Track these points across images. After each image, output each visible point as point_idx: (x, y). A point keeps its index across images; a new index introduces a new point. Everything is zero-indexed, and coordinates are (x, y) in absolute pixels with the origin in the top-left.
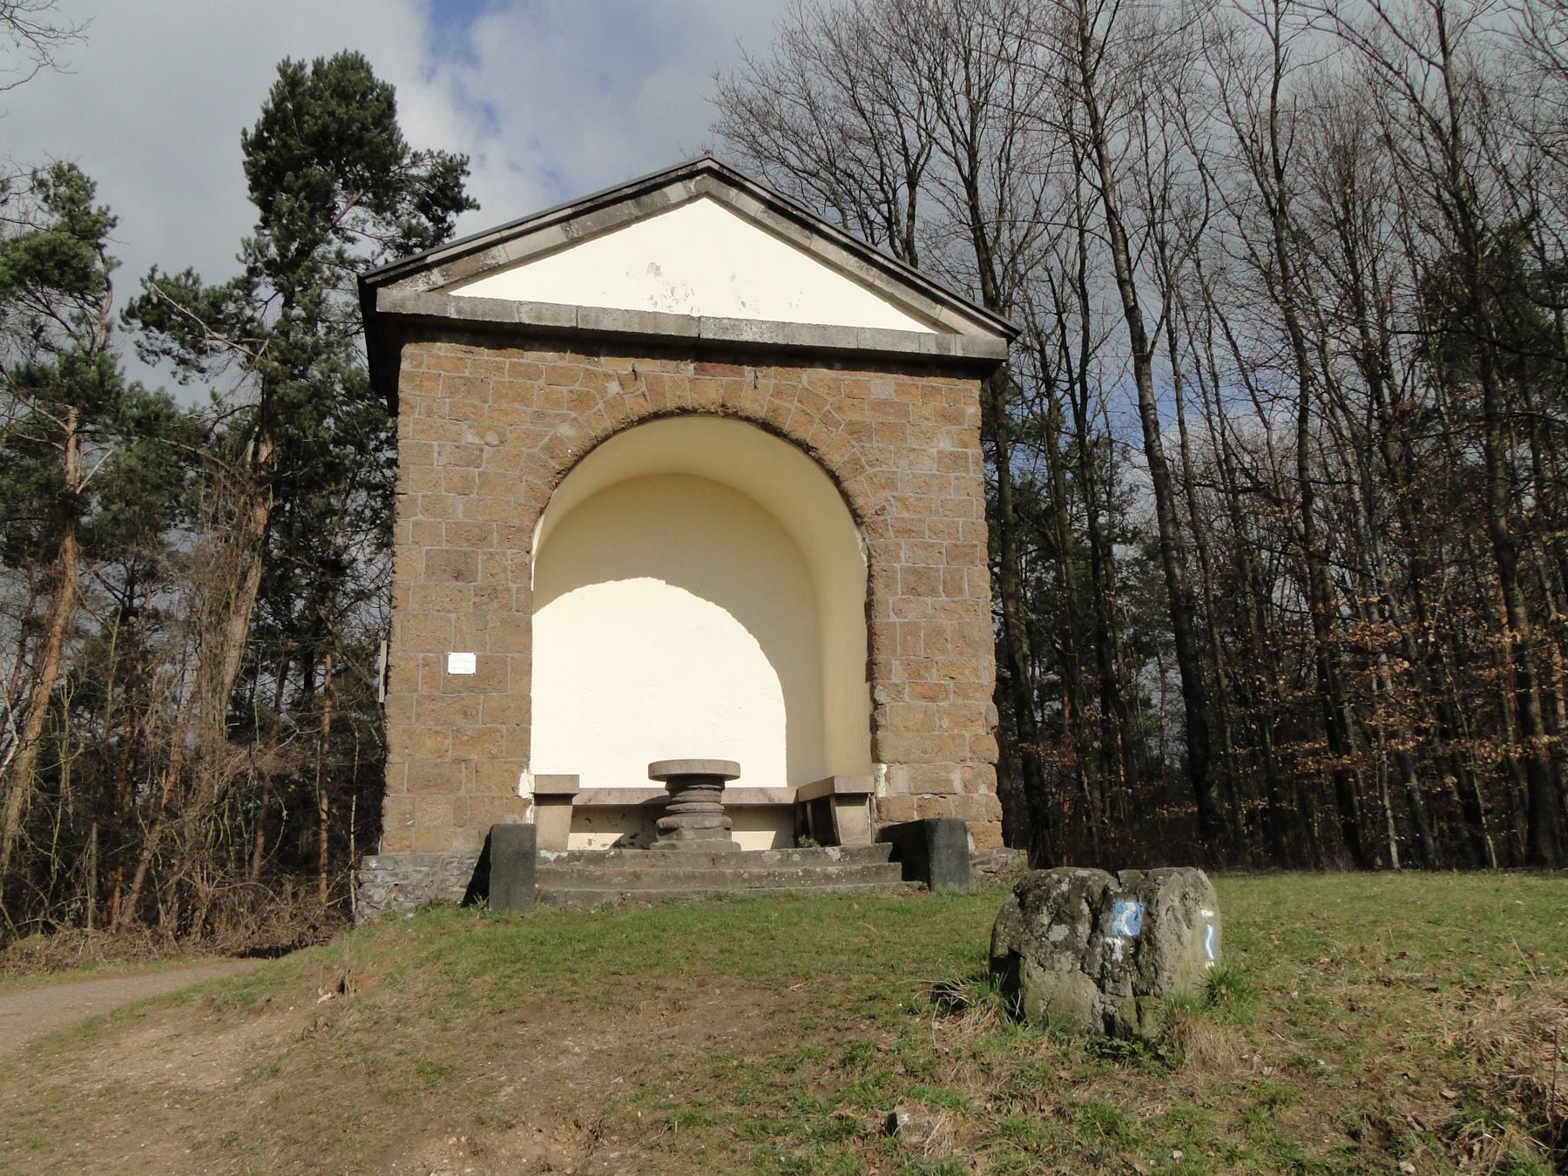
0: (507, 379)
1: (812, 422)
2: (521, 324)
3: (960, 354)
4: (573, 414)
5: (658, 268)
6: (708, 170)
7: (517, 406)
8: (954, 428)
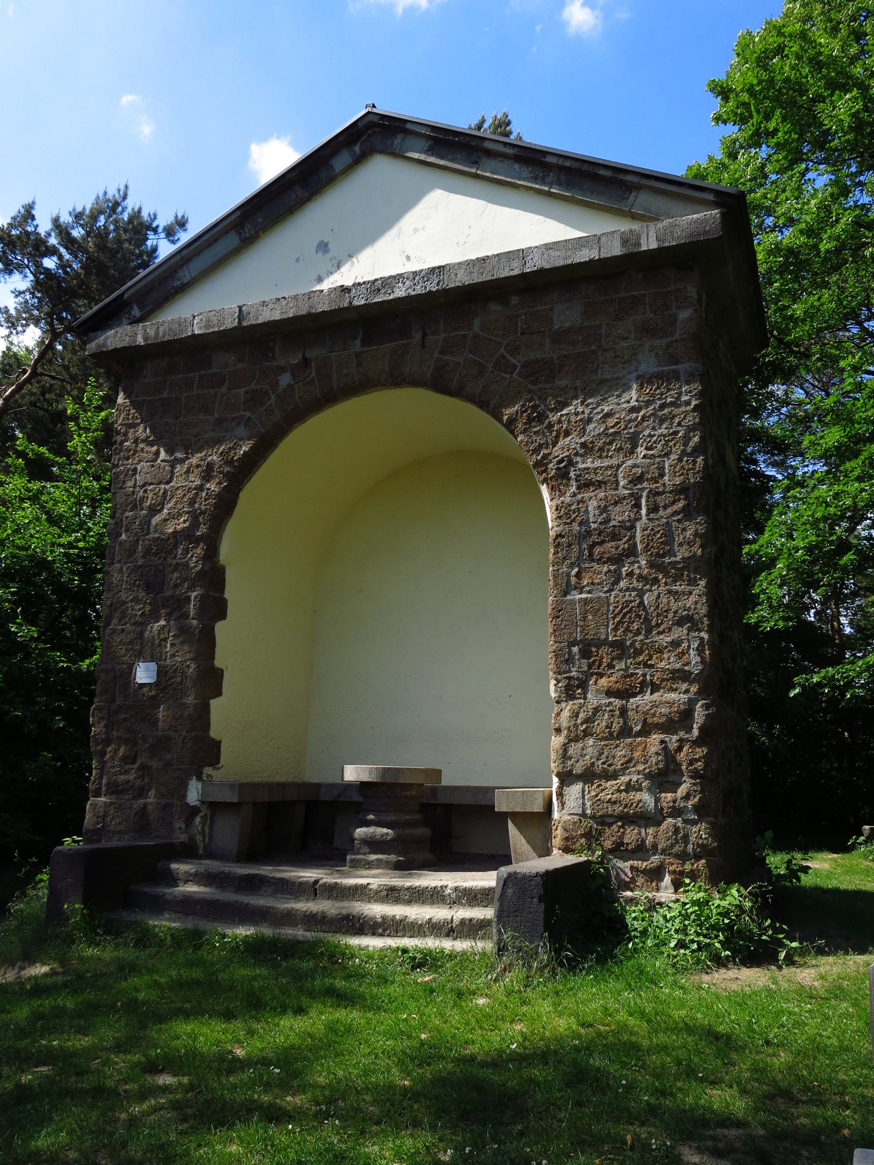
2: (193, 335)
3: (654, 245)
4: (248, 414)
7: (201, 416)
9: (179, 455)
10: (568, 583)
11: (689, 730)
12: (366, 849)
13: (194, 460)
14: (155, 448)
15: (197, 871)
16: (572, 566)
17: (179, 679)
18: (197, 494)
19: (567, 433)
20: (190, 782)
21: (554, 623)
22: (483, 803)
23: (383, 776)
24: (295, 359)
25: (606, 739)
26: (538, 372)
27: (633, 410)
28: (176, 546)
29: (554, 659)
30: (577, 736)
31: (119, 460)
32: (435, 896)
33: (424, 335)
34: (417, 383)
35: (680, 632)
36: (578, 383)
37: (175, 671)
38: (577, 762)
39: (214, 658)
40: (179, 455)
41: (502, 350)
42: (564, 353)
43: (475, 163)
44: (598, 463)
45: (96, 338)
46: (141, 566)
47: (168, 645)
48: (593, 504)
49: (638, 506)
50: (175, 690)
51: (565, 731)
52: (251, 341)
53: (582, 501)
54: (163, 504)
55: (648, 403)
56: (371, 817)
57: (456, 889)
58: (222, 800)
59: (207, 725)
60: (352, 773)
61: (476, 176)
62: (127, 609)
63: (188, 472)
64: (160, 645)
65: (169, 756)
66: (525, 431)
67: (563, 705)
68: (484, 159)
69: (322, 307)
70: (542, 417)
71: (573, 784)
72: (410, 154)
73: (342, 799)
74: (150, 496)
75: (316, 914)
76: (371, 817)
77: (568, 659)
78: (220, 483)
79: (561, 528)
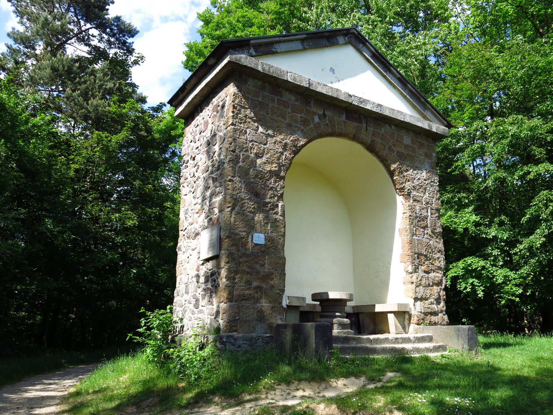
0: (276, 105)
1: (385, 148)
2: (287, 81)
4: (302, 127)
5: (333, 70)
6: (353, 34)
7: (280, 119)
8: (430, 161)
9: (270, 132)
11: (442, 286)
13: (279, 138)
14: (256, 124)
16: (414, 227)
19: (409, 181)
24: (321, 112)
25: (424, 287)
27: (425, 180)
28: (270, 178)
31: (236, 122)
33: (367, 126)
34: (362, 143)
35: (438, 255)
40: (270, 132)
43: (386, 72)
44: (417, 194)
45: (235, 54)
46: (252, 183)
48: (417, 208)
49: (427, 211)
52: (307, 96)
54: (263, 155)
55: (429, 179)
56: (337, 314)
57: (414, 337)
61: (384, 77)
62: (245, 203)
63: (275, 143)
64: (264, 226)
65: (272, 283)
66: (398, 176)
68: (388, 72)
69: (342, 98)
70: (402, 172)
72: (364, 53)
74: (256, 148)
76: (337, 314)
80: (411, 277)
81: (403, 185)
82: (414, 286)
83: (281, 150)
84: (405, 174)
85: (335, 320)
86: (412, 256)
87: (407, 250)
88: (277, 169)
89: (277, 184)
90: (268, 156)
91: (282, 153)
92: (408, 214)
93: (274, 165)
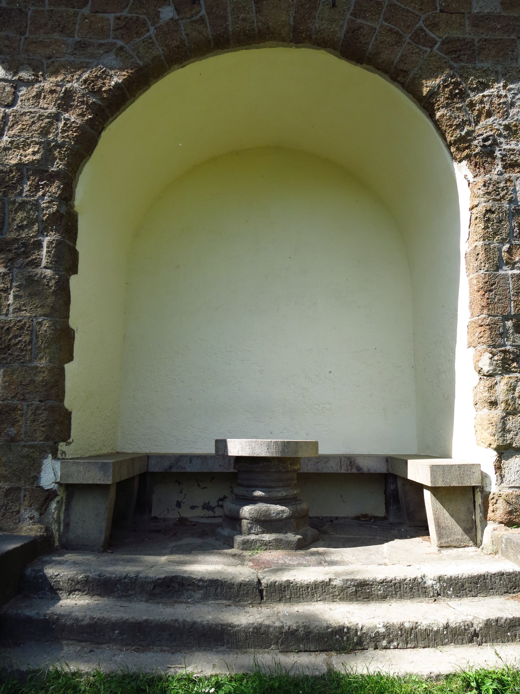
7: (56, 36)
9: (25, 75)
10: (500, 258)
12: (258, 529)
13: (47, 84)
15: (87, 577)
16: (503, 242)
17: (27, 338)
18: (51, 124)
19: (489, 114)
20: (45, 461)
21: (486, 296)
22: (325, 471)
23: (283, 451)
26: (460, 50)
28: (21, 181)
29: (488, 333)
30: (515, 409)
32: (411, 589)
34: (322, 43)
36: (499, 68)
37: (22, 328)
38: (516, 435)
39: (68, 317)
40: (25, 75)
41: (421, 24)
42: (484, 36)
47: (11, 297)
50: (22, 350)
51: (503, 405)
53: (509, 180)
56: (258, 493)
57: (440, 579)
58: (90, 482)
59: (61, 395)
60: (237, 448)
63: (38, 96)
65: (13, 431)
66: (447, 106)
67: (498, 378)
70: (463, 95)
71: (512, 457)
73: (174, 470)
75: (297, 630)
76: (258, 493)
77: (502, 333)
78: (82, 115)
79: (490, 204)
80: (491, 387)
81: (467, 128)
82: (498, 413)
83: (54, 110)
84: (477, 97)
85: (247, 510)
86: (492, 327)
87: (477, 310)
88: (37, 157)
89: (40, 193)
90: (15, 130)
91: (56, 117)
92: (481, 208)
93: (31, 150)
